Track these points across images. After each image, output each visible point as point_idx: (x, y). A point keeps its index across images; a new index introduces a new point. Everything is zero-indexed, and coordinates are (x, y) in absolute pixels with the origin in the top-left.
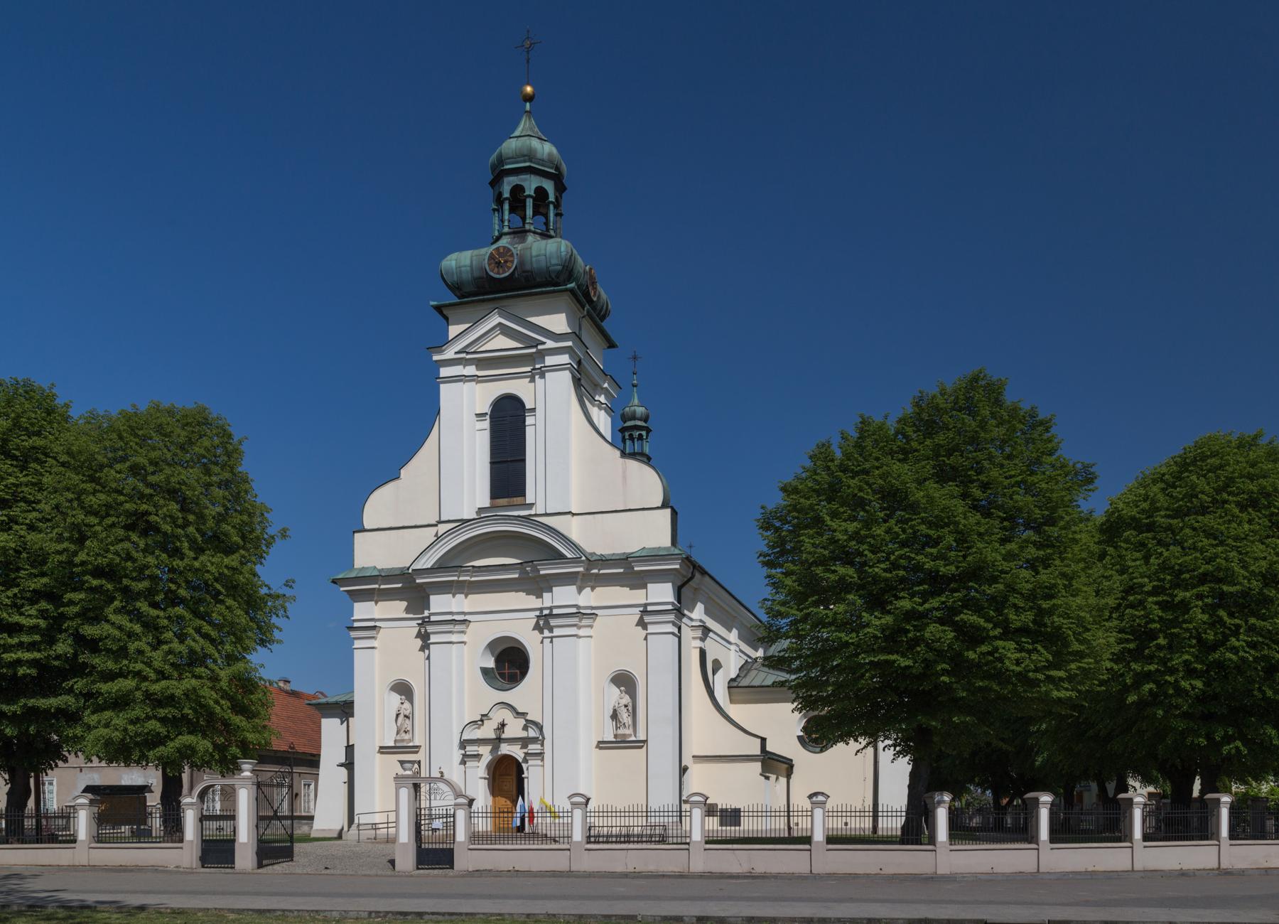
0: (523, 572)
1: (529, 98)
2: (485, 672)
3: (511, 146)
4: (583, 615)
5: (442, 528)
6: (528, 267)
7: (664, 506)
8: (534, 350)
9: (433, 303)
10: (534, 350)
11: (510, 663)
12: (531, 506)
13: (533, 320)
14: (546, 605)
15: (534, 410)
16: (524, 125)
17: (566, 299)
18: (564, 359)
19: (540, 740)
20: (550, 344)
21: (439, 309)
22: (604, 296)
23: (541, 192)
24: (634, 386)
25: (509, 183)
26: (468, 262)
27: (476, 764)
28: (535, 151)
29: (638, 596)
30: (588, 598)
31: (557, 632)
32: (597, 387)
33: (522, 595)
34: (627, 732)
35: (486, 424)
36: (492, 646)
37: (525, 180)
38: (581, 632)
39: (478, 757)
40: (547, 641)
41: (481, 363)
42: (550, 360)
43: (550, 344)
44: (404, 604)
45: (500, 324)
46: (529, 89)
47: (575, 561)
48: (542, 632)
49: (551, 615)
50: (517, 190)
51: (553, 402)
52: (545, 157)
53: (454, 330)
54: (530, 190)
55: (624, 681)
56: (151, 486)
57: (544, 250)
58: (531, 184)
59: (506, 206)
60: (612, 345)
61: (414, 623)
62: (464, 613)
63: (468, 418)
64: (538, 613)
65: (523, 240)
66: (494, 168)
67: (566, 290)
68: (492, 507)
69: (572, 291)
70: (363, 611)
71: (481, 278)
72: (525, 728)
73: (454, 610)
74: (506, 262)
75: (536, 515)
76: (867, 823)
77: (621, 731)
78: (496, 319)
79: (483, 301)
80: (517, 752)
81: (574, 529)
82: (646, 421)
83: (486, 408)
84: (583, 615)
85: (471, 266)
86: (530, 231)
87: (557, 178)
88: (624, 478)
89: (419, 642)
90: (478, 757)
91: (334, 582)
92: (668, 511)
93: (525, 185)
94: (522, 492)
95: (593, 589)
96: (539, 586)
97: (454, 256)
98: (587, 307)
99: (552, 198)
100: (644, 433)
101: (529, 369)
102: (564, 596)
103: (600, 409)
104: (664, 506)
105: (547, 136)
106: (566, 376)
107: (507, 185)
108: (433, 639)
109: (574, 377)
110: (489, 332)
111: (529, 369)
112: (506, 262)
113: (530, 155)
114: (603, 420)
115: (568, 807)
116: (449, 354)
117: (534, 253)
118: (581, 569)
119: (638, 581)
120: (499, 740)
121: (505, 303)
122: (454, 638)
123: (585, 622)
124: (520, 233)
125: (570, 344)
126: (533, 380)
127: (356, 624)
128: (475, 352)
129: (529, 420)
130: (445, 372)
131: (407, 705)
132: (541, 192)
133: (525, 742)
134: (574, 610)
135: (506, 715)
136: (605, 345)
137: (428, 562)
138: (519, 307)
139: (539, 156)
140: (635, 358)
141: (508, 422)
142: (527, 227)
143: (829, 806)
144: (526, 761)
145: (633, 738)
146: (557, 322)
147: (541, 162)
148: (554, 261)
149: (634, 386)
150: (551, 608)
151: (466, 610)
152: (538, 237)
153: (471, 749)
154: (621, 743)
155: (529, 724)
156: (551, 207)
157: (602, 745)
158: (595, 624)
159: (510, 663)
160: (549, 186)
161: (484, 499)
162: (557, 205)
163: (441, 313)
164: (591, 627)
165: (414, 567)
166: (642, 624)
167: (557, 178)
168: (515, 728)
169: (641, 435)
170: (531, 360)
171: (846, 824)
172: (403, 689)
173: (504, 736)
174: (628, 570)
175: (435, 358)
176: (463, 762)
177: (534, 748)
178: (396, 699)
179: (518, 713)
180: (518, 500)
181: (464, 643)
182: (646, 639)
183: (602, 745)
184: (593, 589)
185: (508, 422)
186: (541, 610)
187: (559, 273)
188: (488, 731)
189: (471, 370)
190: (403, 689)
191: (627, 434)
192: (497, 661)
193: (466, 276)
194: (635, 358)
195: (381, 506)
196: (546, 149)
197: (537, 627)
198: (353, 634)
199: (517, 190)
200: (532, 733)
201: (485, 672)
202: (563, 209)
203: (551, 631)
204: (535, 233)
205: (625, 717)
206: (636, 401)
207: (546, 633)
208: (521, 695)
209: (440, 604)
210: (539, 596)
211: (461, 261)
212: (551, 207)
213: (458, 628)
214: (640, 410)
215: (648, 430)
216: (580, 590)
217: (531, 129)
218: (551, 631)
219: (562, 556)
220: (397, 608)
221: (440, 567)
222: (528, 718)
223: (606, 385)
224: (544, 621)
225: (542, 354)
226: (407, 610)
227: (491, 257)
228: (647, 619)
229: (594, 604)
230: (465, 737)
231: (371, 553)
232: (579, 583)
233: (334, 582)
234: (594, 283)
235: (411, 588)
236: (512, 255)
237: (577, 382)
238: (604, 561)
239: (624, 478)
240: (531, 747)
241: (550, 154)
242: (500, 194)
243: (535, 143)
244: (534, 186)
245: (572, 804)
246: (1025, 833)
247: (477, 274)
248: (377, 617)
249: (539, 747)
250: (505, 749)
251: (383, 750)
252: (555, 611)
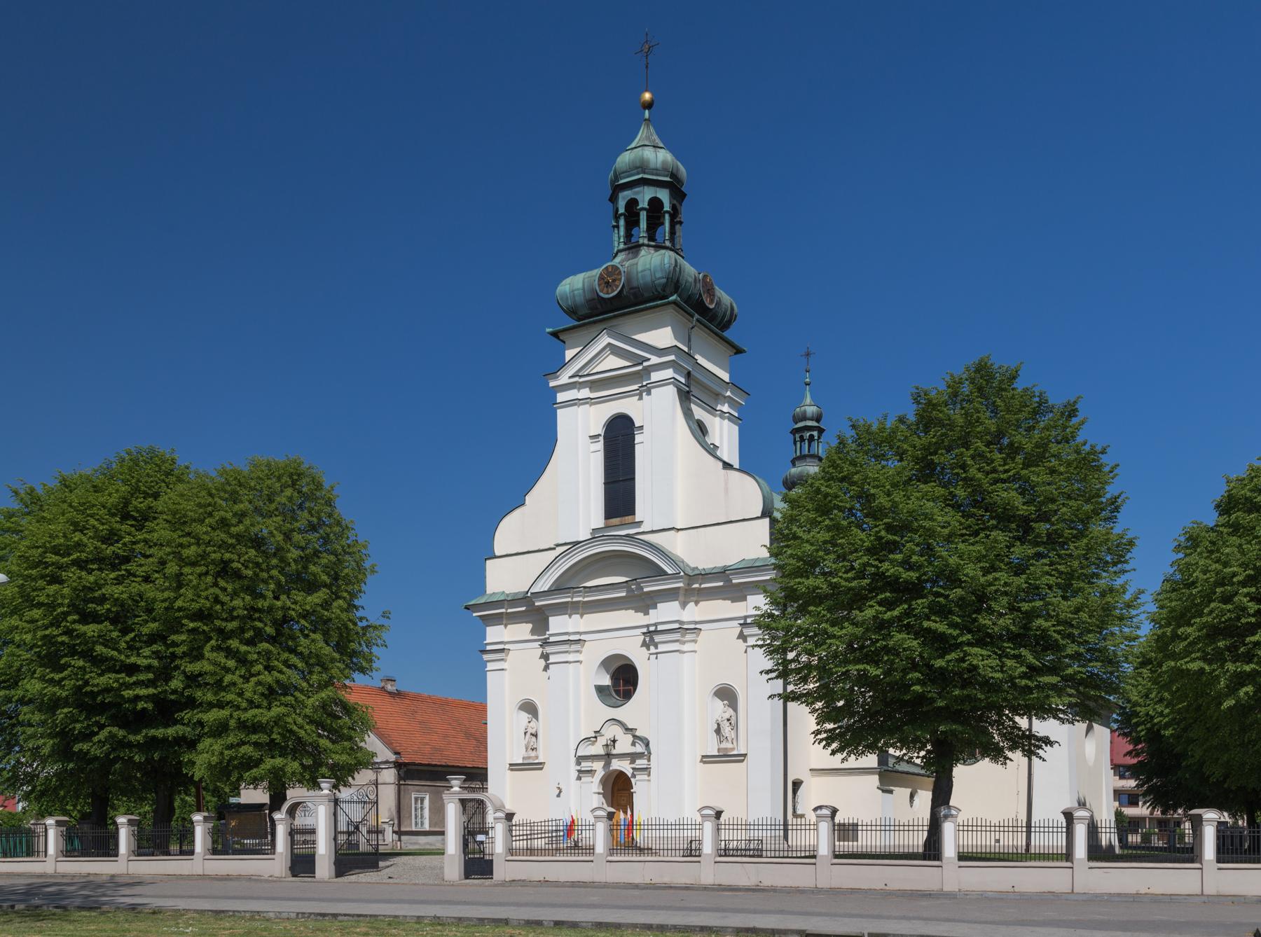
0: (629, 590)
1: (649, 106)
2: (600, 690)
3: (625, 159)
4: (684, 630)
5: (560, 550)
6: (635, 284)
7: (764, 515)
8: (640, 368)
9: (548, 330)
10: (640, 368)
11: (623, 680)
16: (643, 134)
17: (670, 310)
18: (669, 373)
19: (647, 755)
20: (655, 360)
21: (555, 334)
22: (726, 299)
23: (655, 203)
24: (807, 384)
26: (580, 285)
27: (589, 779)
28: (648, 161)
30: (692, 612)
31: (662, 648)
32: (718, 397)
33: (631, 612)
34: (729, 745)
35: (600, 445)
36: (606, 663)
37: (637, 193)
38: (686, 647)
39: (591, 772)
41: (594, 385)
42: (656, 376)
43: (655, 360)
44: (530, 626)
45: (609, 344)
46: (647, 96)
47: (675, 576)
49: (657, 632)
50: (632, 203)
51: (658, 415)
52: (659, 166)
53: (569, 354)
54: (644, 203)
55: (726, 694)
56: (232, 536)
57: (651, 262)
58: (645, 196)
59: (622, 222)
60: (739, 351)
61: (537, 644)
62: (580, 633)
63: (583, 440)
64: (645, 630)
65: (636, 255)
66: (613, 182)
67: (669, 303)
68: (607, 527)
69: (674, 303)
70: (494, 634)
72: (633, 744)
73: (571, 630)
74: (614, 281)
75: (643, 533)
76: (1021, 840)
77: (724, 745)
78: (605, 340)
79: (595, 322)
80: (625, 766)
81: (678, 545)
82: (818, 420)
83: (600, 430)
84: (684, 630)
86: (643, 245)
87: (675, 186)
88: (727, 490)
89: (543, 662)
90: (591, 772)
91: (467, 608)
92: (767, 520)
93: (638, 197)
94: (632, 511)
95: (697, 603)
96: (645, 603)
97: (568, 280)
98: (697, 316)
99: (667, 207)
100: (815, 433)
101: (636, 387)
102: (667, 612)
103: (722, 417)
104: (764, 515)
106: (671, 391)
107: (624, 197)
108: (552, 659)
109: (680, 391)
110: (598, 354)
111: (636, 387)
112: (614, 281)
113: (642, 166)
114: (724, 433)
115: (699, 820)
116: (564, 378)
117: (640, 269)
118: (681, 585)
119: (738, 593)
120: (608, 757)
121: (615, 322)
122: (571, 657)
123: (689, 637)
124: (633, 248)
125: (672, 357)
126: (641, 398)
127: (489, 648)
128: (588, 375)
129: (638, 439)
130: (561, 397)
131: (730, 712)
132: (655, 203)
133: (633, 757)
134: (677, 626)
135: (616, 731)
136: (731, 352)
137: (544, 585)
138: (626, 325)
139: (652, 166)
140: (808, 355)
141: (619, 439)
142: (641, 241)
143: (960, 820)
144: (634, 776)
145: (735, 752)
146: (663, 337)
147: (655, 171)
148: (659, 275)
149: (807, 384)
150: (656, 625)
151: (582, 630)
152: (652, 250)
153: (586, 765)
154: (725, 757)
155: (637, 739)
156: (667, 216)
157: (706, 759)
158: (584, 650)
159: (623, 680)
160: (664, 195)
161: (598, 520)
162: (674, 213)
163: (558, 338)
164: (695, 641)
165: (534, 590)
167: (675, 186)
168: (624, 744)
169: (812, 437)
170: (637, 379)
171: (998, 841)
172: (530, 708)
173: (614, 752)
174: (725, 583)
175: (552, 384)
176: (579, 778)
177: (641, 763)
178: (525, 716)
179: (627, 729)
180: (628, 519)
181: (580, 662)
183: (706, 759)
184: (697, 603)
185: (619, 439)
186: (648, 626)
187: (665, 286)
188: (598, 749)
189: (585, 393)
190: (530, 708)
191: (797, 436)
192: (612, 678)
193: (580, 299)
194: (808, 355)
195: (510, 532)
196: (660, 157)
197: (645, 645)
198: (486, 657)
199: (632, 203)
200: (639, 748)
201: (600, 690)
202: (683, 216)
203: (656, 647)
204: (648, 246)
205: (726, 730)
206: (808, 400)
207: (653, 649)
208: (629, 712)
209: (559, 625)
210: (646, 613)
211: (574, 285)
212: (667, 216)
213: (574, 647)
214: (811, 410)
215: (821, 431)
216: (684, 605)
217: (648, 138)
218: (656, 647)
220: (523, 630)
221: (557, 589)
222: (637, 733)
223: (728, 394)
224: (651, 637)
226: (533, 632)
227: (601, 278)
229: (697, 619)
230: (579, 754)
231: (502, 578)
232: (681, 598)
233: (467, 608)
234: (710, 292)
235: (532, 610)
236: (620, 273)
237: (685, 396)
239: (727, 490)
240: (638, 762)
241: (664, 163)
242: (617, 210)
243: (649, 153)
244: (647, 198)
245: (703, 816)
246: (1190, 854)
247: (588, 296)
248: (506, 640)
249: (645, 762)
250: (616, 765)
251: (514, 767)
252: (660, 628)
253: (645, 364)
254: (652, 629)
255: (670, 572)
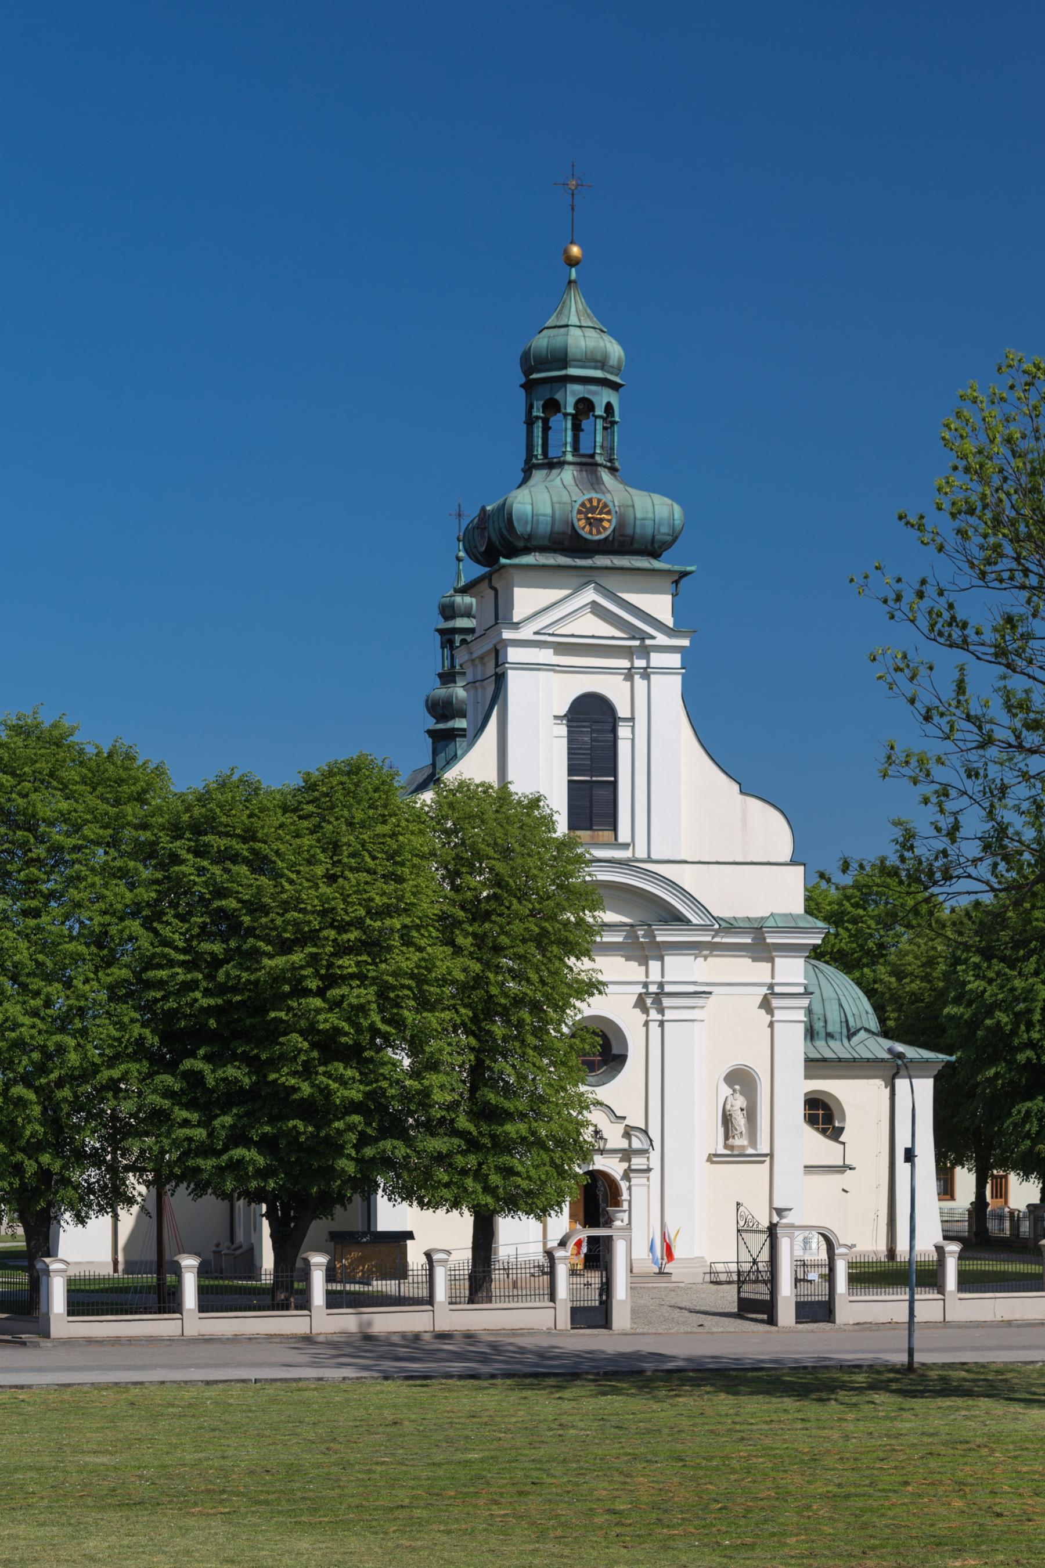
10: (637, 643)
12: (626, 846)
13: (620, 594)
14: (651, 979)
15: (632, 719)
16: (575, 308)
25: (573, 393)
29: (760, 971)
37: (595, 393)
40: (654, 1027)
42: (657, 659)
43: (661, 639)
45: (594, 602)
48: (645, 1011)
50: (585, 406)
64: (640, 989)
71: (564, 533)
72: (627, 1135)
78: (590, 595)
85: (553, 517)
86: (601, 465)
88: (744, 821)
102: (680, 969)
105: (609, 326)
106: (676, 681)
128: (553, 635)
138: (610, 582)
150: (661, 985)
166: (766, 1004)
174: (757, 940)
182: (771, 1025)
184: (706, 958)
186: (646, 985)
199: (585, 406)
203: (661, 1011)
207: (654, 1014)
218: (661, 1011)
219: (688, 922)
222: (626, 1122)
224: (652, 1000)
225: (645, 652)
228: (775, 1002)
238: (729, 926)
239: (744, 821)
253: (648, 642)
254: (653, 989)
255: (695, 921)
